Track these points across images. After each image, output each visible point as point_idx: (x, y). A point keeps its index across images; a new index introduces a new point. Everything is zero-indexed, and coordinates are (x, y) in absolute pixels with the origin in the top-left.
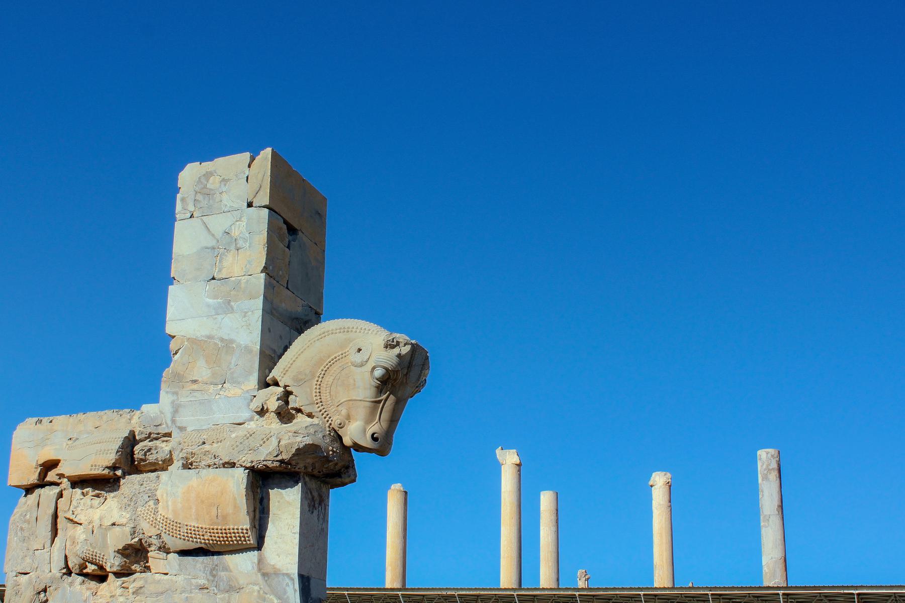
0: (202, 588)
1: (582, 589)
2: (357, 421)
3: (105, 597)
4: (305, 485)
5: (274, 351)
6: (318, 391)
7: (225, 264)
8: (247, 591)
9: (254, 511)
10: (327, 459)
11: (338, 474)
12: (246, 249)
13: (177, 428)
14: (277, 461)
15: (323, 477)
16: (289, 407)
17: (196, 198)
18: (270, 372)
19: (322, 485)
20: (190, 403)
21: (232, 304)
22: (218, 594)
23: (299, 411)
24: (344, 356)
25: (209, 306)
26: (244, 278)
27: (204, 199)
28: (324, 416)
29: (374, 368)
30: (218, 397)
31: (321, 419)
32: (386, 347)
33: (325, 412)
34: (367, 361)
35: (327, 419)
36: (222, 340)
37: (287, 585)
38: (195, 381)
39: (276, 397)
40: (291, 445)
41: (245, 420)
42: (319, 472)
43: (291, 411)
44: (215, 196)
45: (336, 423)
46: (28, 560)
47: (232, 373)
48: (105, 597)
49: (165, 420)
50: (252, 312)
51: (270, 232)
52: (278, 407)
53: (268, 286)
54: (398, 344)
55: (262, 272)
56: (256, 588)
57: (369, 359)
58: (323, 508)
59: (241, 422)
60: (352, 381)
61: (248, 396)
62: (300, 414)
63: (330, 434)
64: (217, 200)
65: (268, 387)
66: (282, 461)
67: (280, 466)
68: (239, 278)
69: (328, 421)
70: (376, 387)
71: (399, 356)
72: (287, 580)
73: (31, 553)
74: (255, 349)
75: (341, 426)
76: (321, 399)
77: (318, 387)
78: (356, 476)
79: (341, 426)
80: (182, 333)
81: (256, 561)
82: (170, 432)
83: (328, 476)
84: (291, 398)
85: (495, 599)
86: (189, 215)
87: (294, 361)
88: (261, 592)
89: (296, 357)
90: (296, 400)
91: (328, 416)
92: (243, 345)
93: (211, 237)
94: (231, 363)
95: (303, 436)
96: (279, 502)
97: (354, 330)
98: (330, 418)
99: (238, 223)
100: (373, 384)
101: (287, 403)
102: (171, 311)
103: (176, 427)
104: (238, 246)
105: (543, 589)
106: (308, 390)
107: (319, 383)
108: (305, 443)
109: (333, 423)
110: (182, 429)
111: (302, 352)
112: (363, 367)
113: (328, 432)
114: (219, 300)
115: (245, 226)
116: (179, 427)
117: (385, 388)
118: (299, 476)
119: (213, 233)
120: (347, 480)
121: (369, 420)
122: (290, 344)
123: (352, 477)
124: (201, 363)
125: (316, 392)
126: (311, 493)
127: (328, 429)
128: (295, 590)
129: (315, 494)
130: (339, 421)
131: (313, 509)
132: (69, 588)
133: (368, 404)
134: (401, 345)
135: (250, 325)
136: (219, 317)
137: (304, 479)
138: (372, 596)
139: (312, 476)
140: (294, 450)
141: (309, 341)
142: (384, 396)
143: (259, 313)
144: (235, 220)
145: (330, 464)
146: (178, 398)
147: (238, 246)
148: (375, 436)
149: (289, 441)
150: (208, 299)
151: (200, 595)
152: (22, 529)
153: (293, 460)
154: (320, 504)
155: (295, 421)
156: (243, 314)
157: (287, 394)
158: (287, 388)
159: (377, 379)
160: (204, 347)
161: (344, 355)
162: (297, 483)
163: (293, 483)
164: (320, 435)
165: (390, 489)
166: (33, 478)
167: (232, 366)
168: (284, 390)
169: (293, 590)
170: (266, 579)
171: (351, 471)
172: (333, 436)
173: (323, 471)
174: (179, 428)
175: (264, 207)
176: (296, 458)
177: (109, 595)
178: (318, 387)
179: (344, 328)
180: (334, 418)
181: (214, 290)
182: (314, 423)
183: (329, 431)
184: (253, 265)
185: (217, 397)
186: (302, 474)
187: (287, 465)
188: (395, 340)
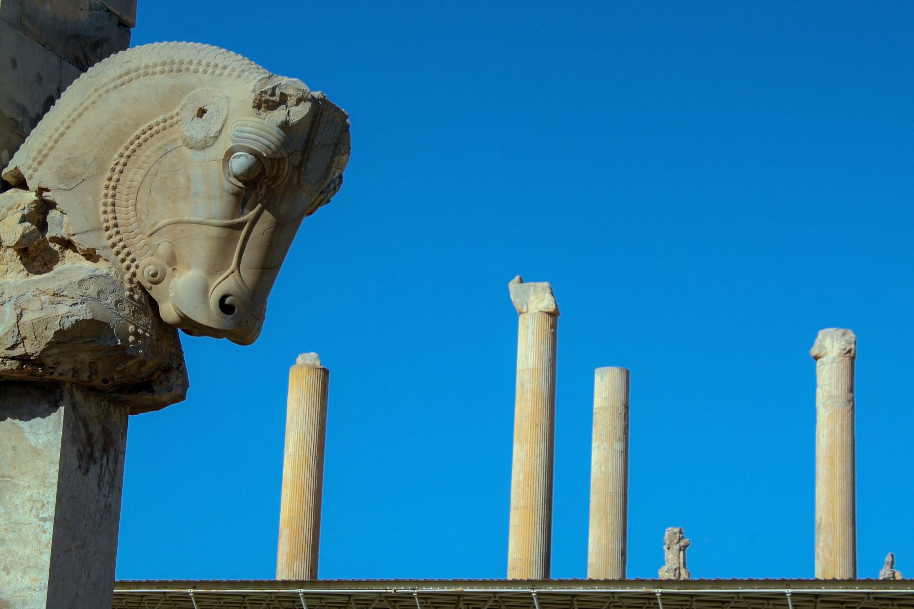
1: (669, 582)
2: (190, 268)
4: (73, 409)
5: (23, 110)
6: (110, 201)
10: (122, 353)
11: (146, 385)
14: (13, 358)
15: (115, 392)
16: (48, 236)
18: (11, 157)
19: (112, 409)
23: (67, 244)
24: (169, 124)
28: (121, 256)
29: (230, 153)
31: (114, 264)
32: (258, 105)
33: (124, 247)
34: (216, 137)
35: (127, 262)
39: (19, 215)
40: (44, 323)
42: (105, 381)
43: (51, 245)
45: (146, 274)
52: (23, 236)
54: (284, 99)
57: (220, 132)
58: (111, 458)
60: (182, 180)
62: (69, 253)
63: (131, 297)
66: (24, 359)
67: (20, 368)
69: (128, 268)
70: (233, 194)
71: (285, 126)
75: (157, 279)
76: (115, 218)
77: (111, 192)
78: (185, 385)
79: (157, 279)
83: (122, 388)
84: (53, 216)
85: (494, 601)
87: (62, 134)
89: (66, 125)
90: (62, 222)
91: (131, 257)
95: (71, 302)
97: (193, 67)
98: (133, 260)
100: (228, 186)
101: (43, 226)
105: (592, 582)
106: (90, 198)
107: (112, 184)
108: (74, 318)
109: (139, 272)
111: (80, 115)
112: (207, 151)
113: (127, 293)
117: (252, 196)
118: (62, 391)
120: (165, 397)
121: (215, 268)
122: (59, 91)
123: (178, 391)
125: (105, 204)
126: (86, 427)
127: (127, 286)
129: (96, 429)
130: (151, 269)
131: (88, 463)
133: (214, 231)
134: (289, 103)
137: (72, 396)
138: (244, 596)
139: (90, 390)
140: (50, 334)
141: (97, 90)
142: (250, 215)
145: (130, 363)
148: (227, 301)
149: (43, 314)
153: (48, 356)
154: (105, 450)
155: (58, 267)
157: (44, 206)
158: (45, 194)
159: (236, 177)
161: (168, 122)
162: (55, 406)
163: (46, 406)
164: (110, 300)
165: (295, 363)
168: (36, 198)
171: (173, 376)
172: (139, 301)
173: (112, 379)
176: (55, 351)
178: (111, 192)
179: (172, 63)
180: (142, 262)
182: (98, 273)
183: (131, 290)
186: (68, 385)
187: (35, 367)
188: (277, 92)
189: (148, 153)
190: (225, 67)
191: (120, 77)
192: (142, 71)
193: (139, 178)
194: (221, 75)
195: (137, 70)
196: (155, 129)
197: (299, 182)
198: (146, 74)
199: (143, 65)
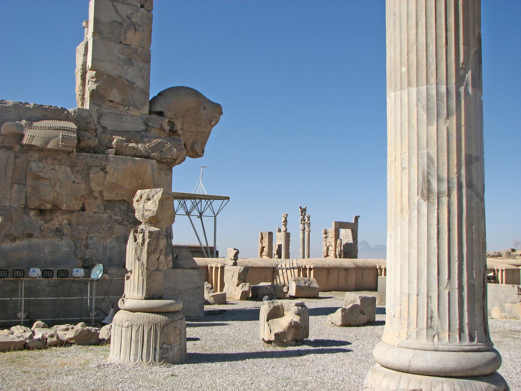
26: (139, 48)
30: (126, 113)
38: (112, 101)
49: (93, 120)
68: (138, 47)
94: (133, 96)
96: (161, 178)
116: (102, 126)
124: (115, 91)
136: (126, 67)
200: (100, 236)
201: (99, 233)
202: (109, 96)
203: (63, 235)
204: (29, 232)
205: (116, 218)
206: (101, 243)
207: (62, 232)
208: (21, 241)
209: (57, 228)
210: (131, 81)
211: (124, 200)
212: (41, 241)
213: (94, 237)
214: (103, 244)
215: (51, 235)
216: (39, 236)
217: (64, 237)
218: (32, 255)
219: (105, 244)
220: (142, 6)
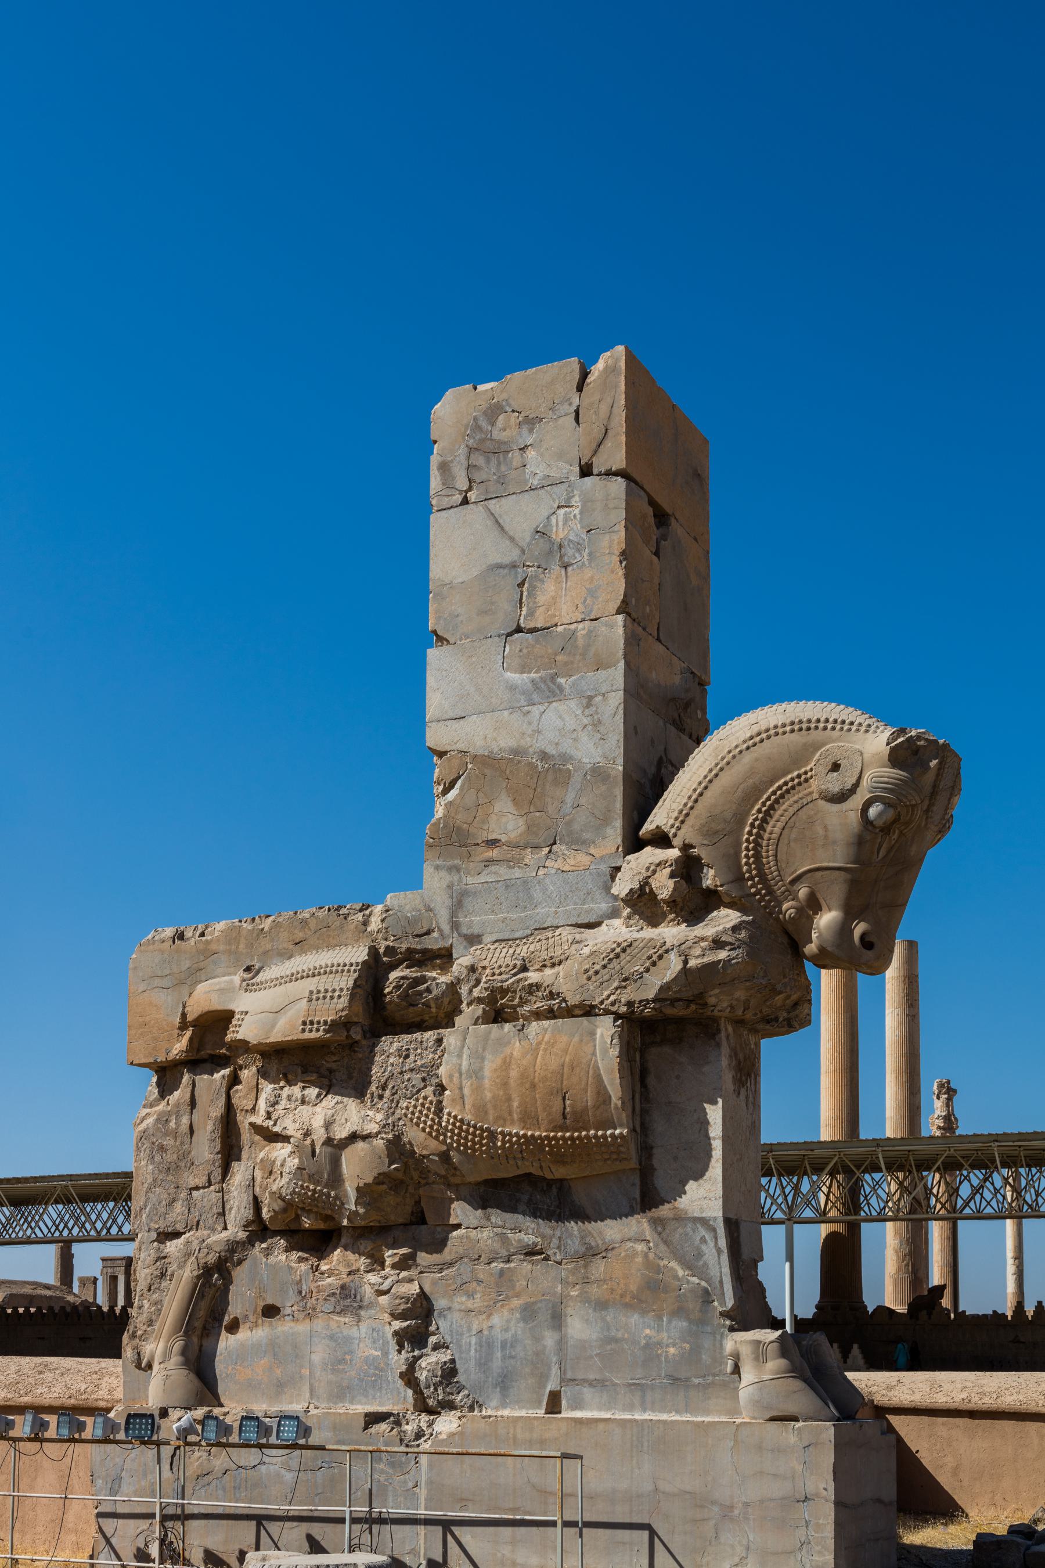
0: (531, 1252)
3: (338, 1275)
7: (541, 598)
8: (623, 1254)
9: (633, 1098)
12: (583, 564)
13: (462, 939)
17: (472, 461)
20: (485, 885)
21: (562, 680)
22: (564, 1261)
25: (512, 688)
26: (581, 626)
27: (488, 461)
36: (544, 756)
37: (703, 1240)
38: (492, 843)
41: (602, 917)
44: (510, 455)
46: (179, 1207)
47: (569, 824)
48: (338, 1275)
50: (603, 695)
51: (630, 526)
53: (632, 641)
55: (618, 612)
56: (640, 1247)
59: (592, 919)
61: (605, 868)
64: (515, 464)
65: (642, 849)
72: (702, 1232)
73: (183, 1195)
74: (613, 773)
80: (461, 746)
81: (637, 1195)
82: (447, 945)
86: (458, 498)
88: (651, 1256)
92: (589, 766)
93: (508, 542)
96: (678, 1077)
99: (562, 511)
102: (435, 702)
103: (460, 935)
104: (566, 559)
110: (473, 940)
114: (533, 675)
115: (578, 517)
116: (465, 935)
119: (511, 533)
124: (504, 805)
128: (719, 1251)
132: (265, 1259)
135: (600, 723)
136: (536, 710)
143: (617, 698)
144: (556, 506)
146: (460, 878)
147: (566, 559)
150: (509, 673)
151: (527, 1266)
152: (162, 1148)
156: (585, 701)
160: (508, 773)
166: (179, 1047)
167: (567, 808)
169: (714, 1250)
170: (659, 1229)
174: (465, 939)
175: (616, 474)
177: (345, 1271)
181: (521, 654)
184: (600, 599)
185: (540, 873)
186: (723, 1019)
189: (784, 807)
190: (852, 723)
191: (751, 738)
192: (772, 732)
193: (777, 830)
194: (850, 730)
195: (767, 730)
196: (790, 784)
197: (926, 824)
198: (777, 734)
199: (772, 726)
200: (470, 1304)
201: (469, 1296)
202: (486, 827)
203: (360, 1307)
204: (270, 1301)
205: (520, 1241)
206: (475, 1328)
207: (358, 1298)
208: (252, 1331)
209: (343, 1287)
210: (554, 752)
211: (528, 1176)
212: (302, 1328)
213: (450, 1308)
214: (481, 1331)
215: (329, 1307)
216: (296, 1314)
217: (362, 1313)
218: (278, 1372)
219: (486, 1332)
220: (586, 471)
